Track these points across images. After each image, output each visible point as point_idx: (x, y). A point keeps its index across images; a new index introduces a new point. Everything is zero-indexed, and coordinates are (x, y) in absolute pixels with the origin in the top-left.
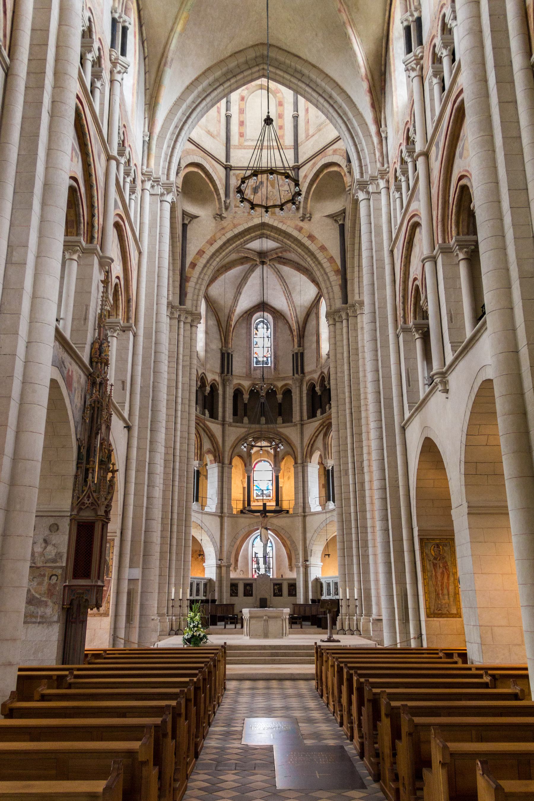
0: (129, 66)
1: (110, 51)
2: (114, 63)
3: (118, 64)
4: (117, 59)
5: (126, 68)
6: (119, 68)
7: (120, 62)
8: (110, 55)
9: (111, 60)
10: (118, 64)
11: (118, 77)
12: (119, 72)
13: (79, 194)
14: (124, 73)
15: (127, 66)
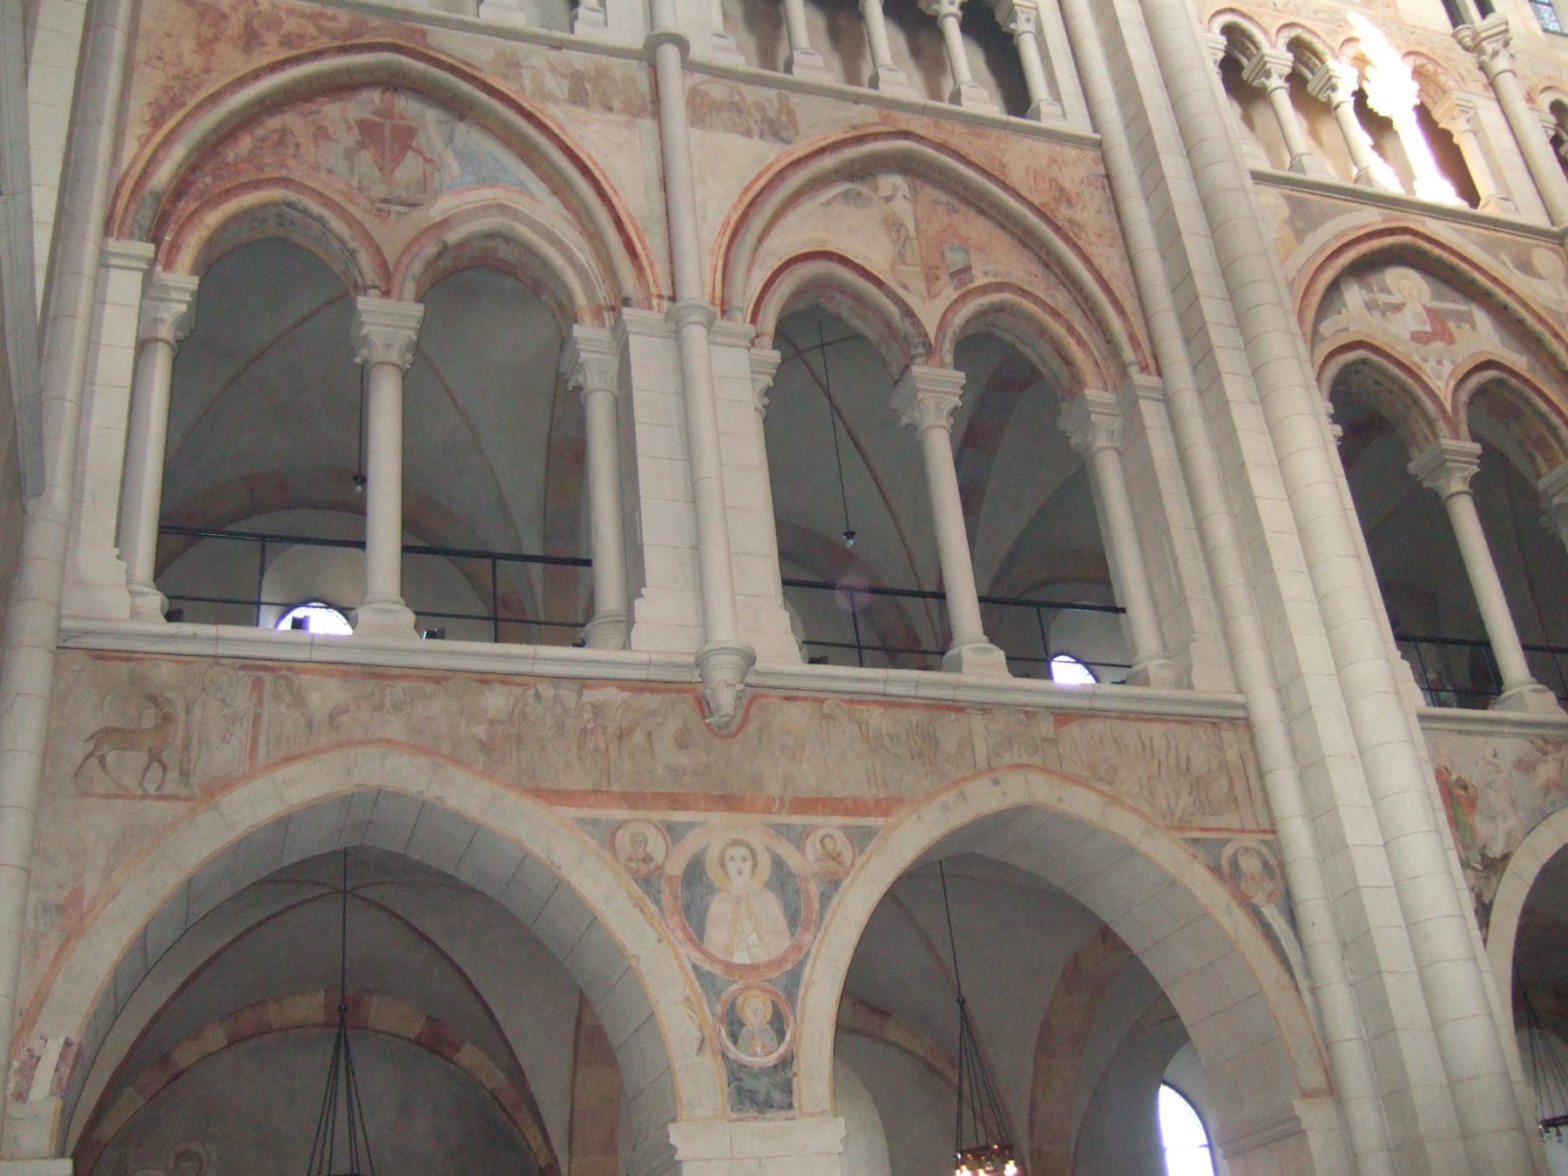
0: (1506, 23)
1: (1454, 36)
2: (1475, 48)
3: (1484, 43)
4: (1475, 35)
5: (1506, 31)
6: (1489, 47)
7: (1483, 35)
8: (1460, 42)
9: (1466, 49)
10: (1484, 43)
11: (1501, 63)
12: (1495, 54)
13: (1514, 382)
14: (1506, 44)
15: (1503, 27)
